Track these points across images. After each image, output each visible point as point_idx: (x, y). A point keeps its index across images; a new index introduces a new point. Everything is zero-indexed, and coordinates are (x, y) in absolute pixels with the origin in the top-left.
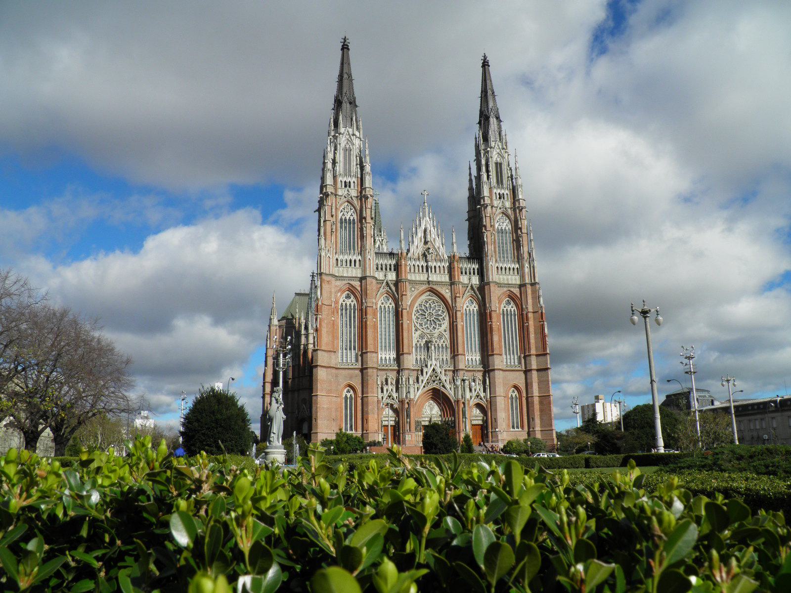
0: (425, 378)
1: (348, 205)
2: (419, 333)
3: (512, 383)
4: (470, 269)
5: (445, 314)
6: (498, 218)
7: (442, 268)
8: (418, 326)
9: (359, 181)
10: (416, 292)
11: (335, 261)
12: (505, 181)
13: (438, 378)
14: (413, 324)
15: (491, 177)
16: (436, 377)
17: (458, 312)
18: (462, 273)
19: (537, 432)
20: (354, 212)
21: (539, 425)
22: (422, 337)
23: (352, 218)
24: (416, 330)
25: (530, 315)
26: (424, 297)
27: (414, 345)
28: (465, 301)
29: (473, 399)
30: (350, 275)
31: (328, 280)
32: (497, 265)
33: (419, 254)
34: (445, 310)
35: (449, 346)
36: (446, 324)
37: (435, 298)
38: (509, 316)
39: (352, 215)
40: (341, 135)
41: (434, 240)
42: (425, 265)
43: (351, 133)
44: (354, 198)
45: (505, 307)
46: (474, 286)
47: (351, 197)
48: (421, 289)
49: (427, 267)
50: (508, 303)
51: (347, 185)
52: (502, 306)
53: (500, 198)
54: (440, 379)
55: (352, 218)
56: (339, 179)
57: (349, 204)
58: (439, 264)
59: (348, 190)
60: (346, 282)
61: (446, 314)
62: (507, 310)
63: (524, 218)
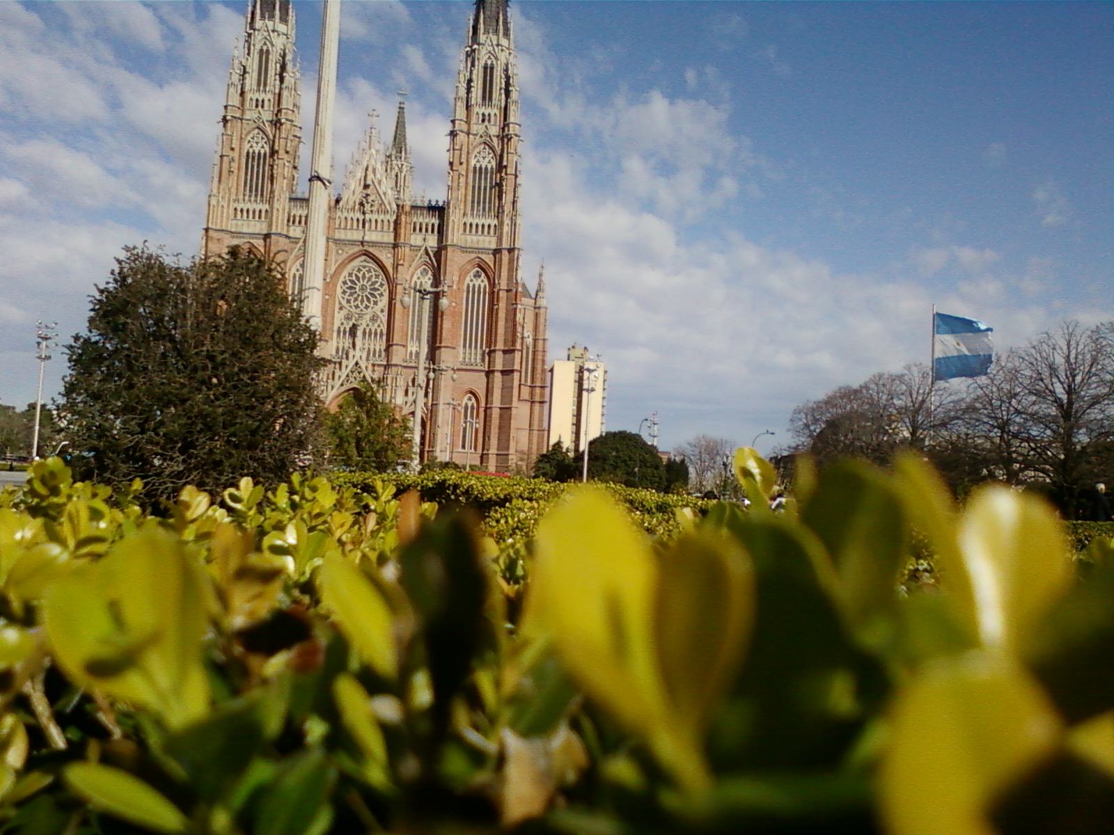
0: (345, 372)
1: (258, 134)
2: (342, 312)
3: (467, 387)
4: (427, 225)
5: (384, 288)
6: (477, 150)
7: (386, 223)
8: (344, 302)
9: (277, 98)
10: (345, 256)
11: (232, 212)
12: (495, 95)
13: (362, 375)
14: (337, 299)
15: (472, 89)
16: (359, 373)
17: (398, 286)
18: (415, 229)
19: (490, 456)
20: (266, 143)
21: (496, 447)
22: (348, 318)
23: (262, 152)
24: (341, 308)
25: (503, 294)
26: (356, 263)
27: (336, 328)
28: (416, 270)
29: (409, 404)
30: (251, 231)
31: (219, 237)
32: (465, 220)
33: (355, 202)
34: (385, 282)
35: (385, 332)
36: (384, 302)
37: (373, 265)
38: (482, 294)
39: (263, 147)
40: (256, 32)
41: (380, 182)
42: (361, 217)
43: (271, 28)
44: (266, 124)
45: (472, 281)
46: (429, 250)
47: (263, 122)
48: (351, 252)
49: (364, 220)
50: (477, 275)
51: (259, 104)
52: (468, 279)
53: (483, 121)
54: (364, 377)
55: (262, 152)
56: (248, 96)
57: (260, 132)
58: (382, 217)
59: (260, 113)
60: (247, 241)
61: (386, 286)
62: (474, 285)
63: (512, 151)
